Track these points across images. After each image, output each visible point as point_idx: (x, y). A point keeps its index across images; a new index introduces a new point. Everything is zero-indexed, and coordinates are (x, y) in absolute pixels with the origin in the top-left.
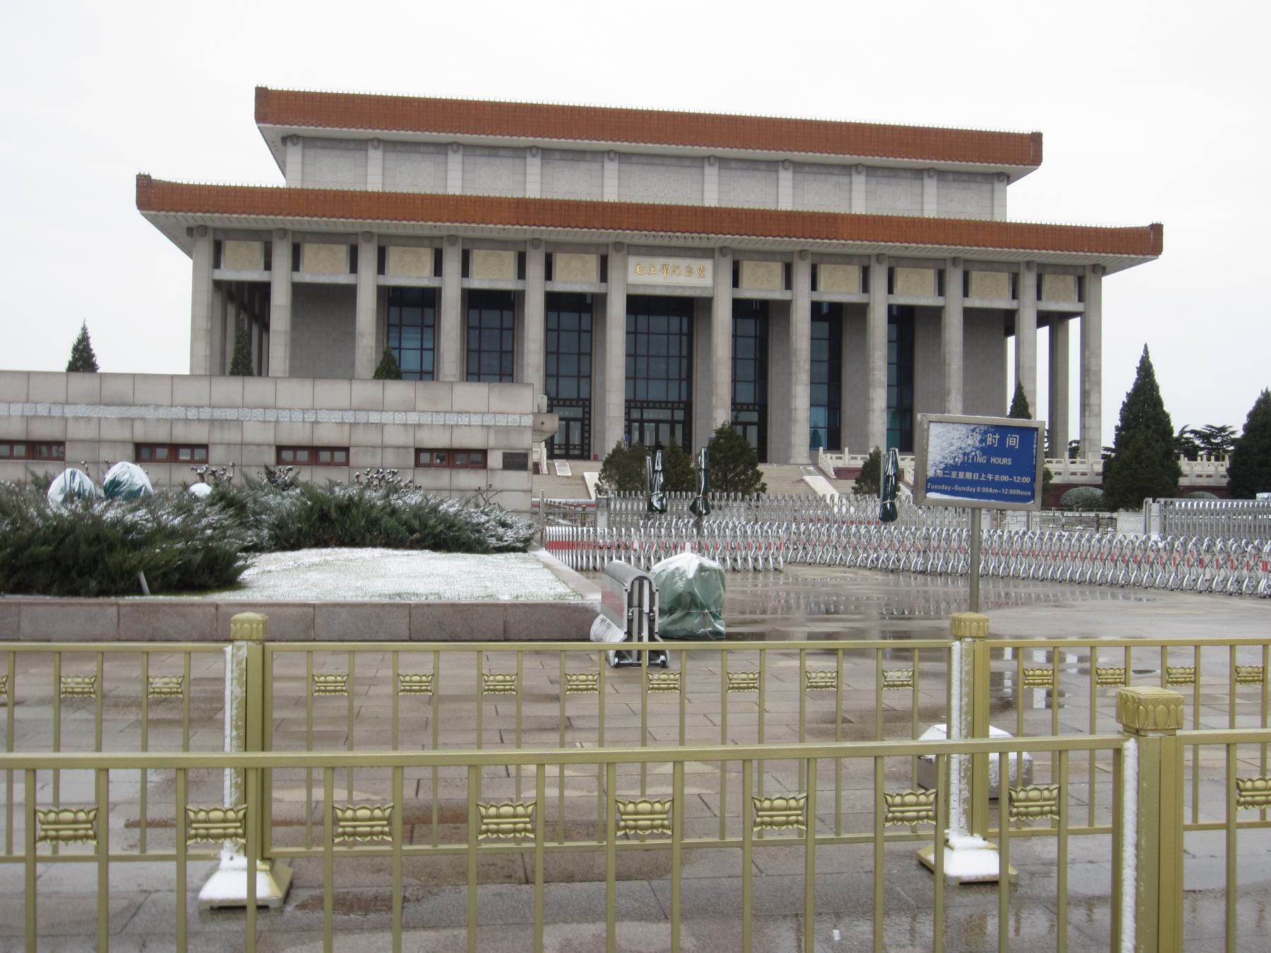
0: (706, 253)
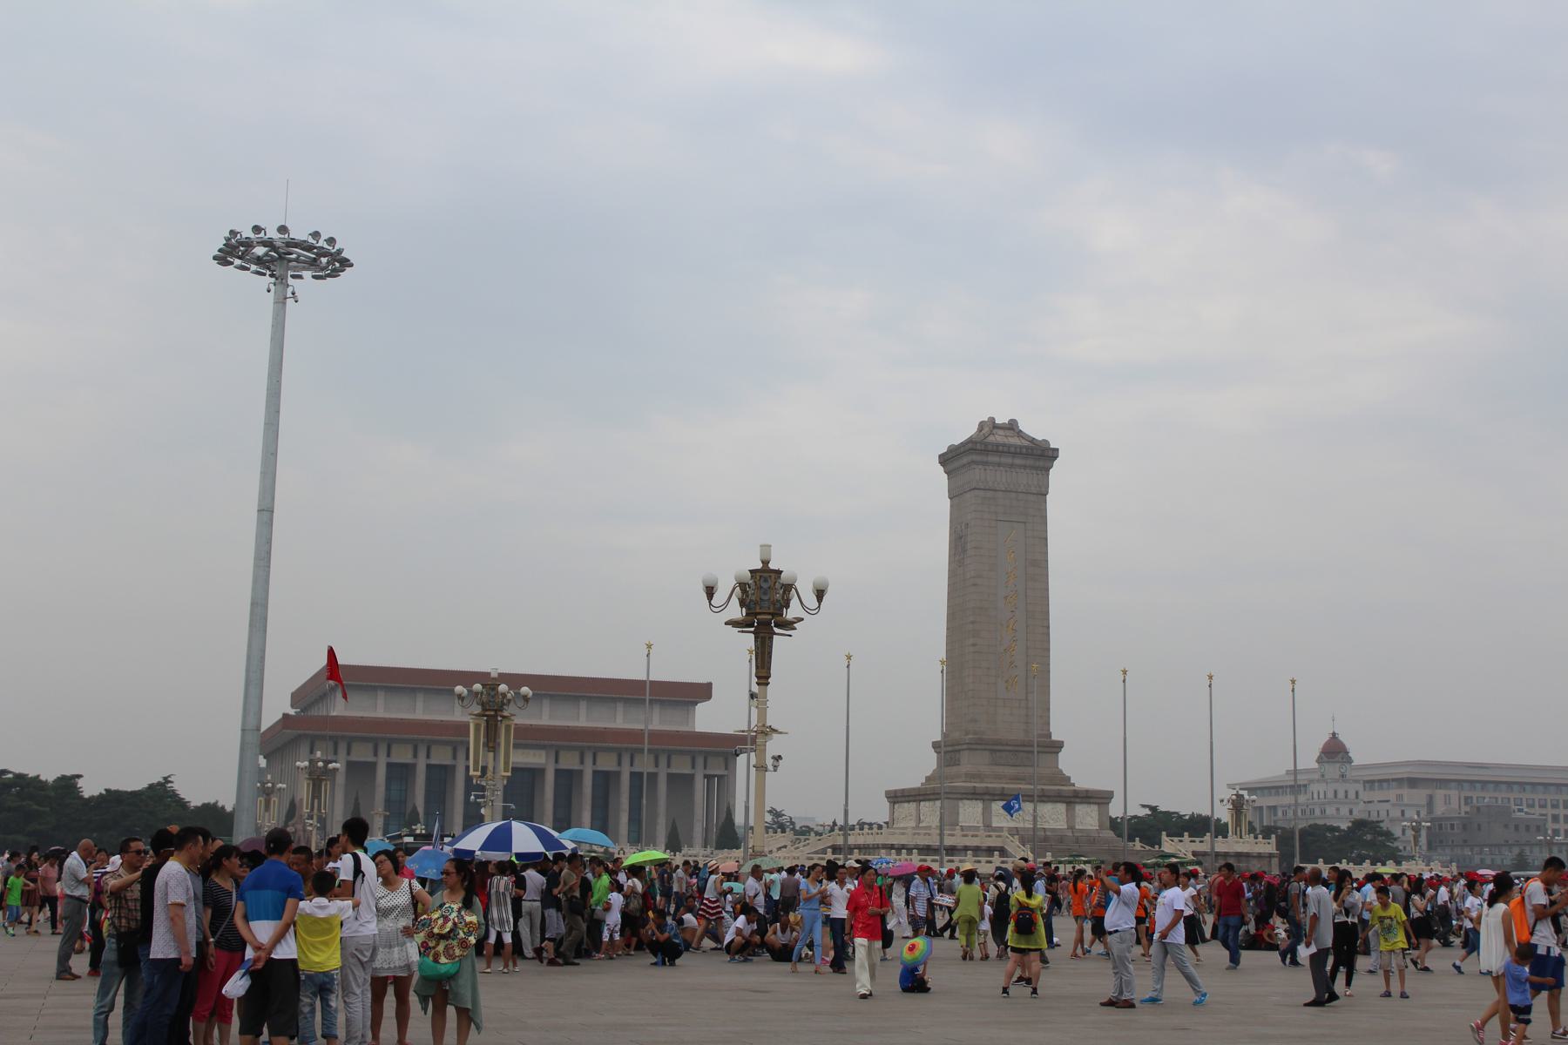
0: (543, 747)
